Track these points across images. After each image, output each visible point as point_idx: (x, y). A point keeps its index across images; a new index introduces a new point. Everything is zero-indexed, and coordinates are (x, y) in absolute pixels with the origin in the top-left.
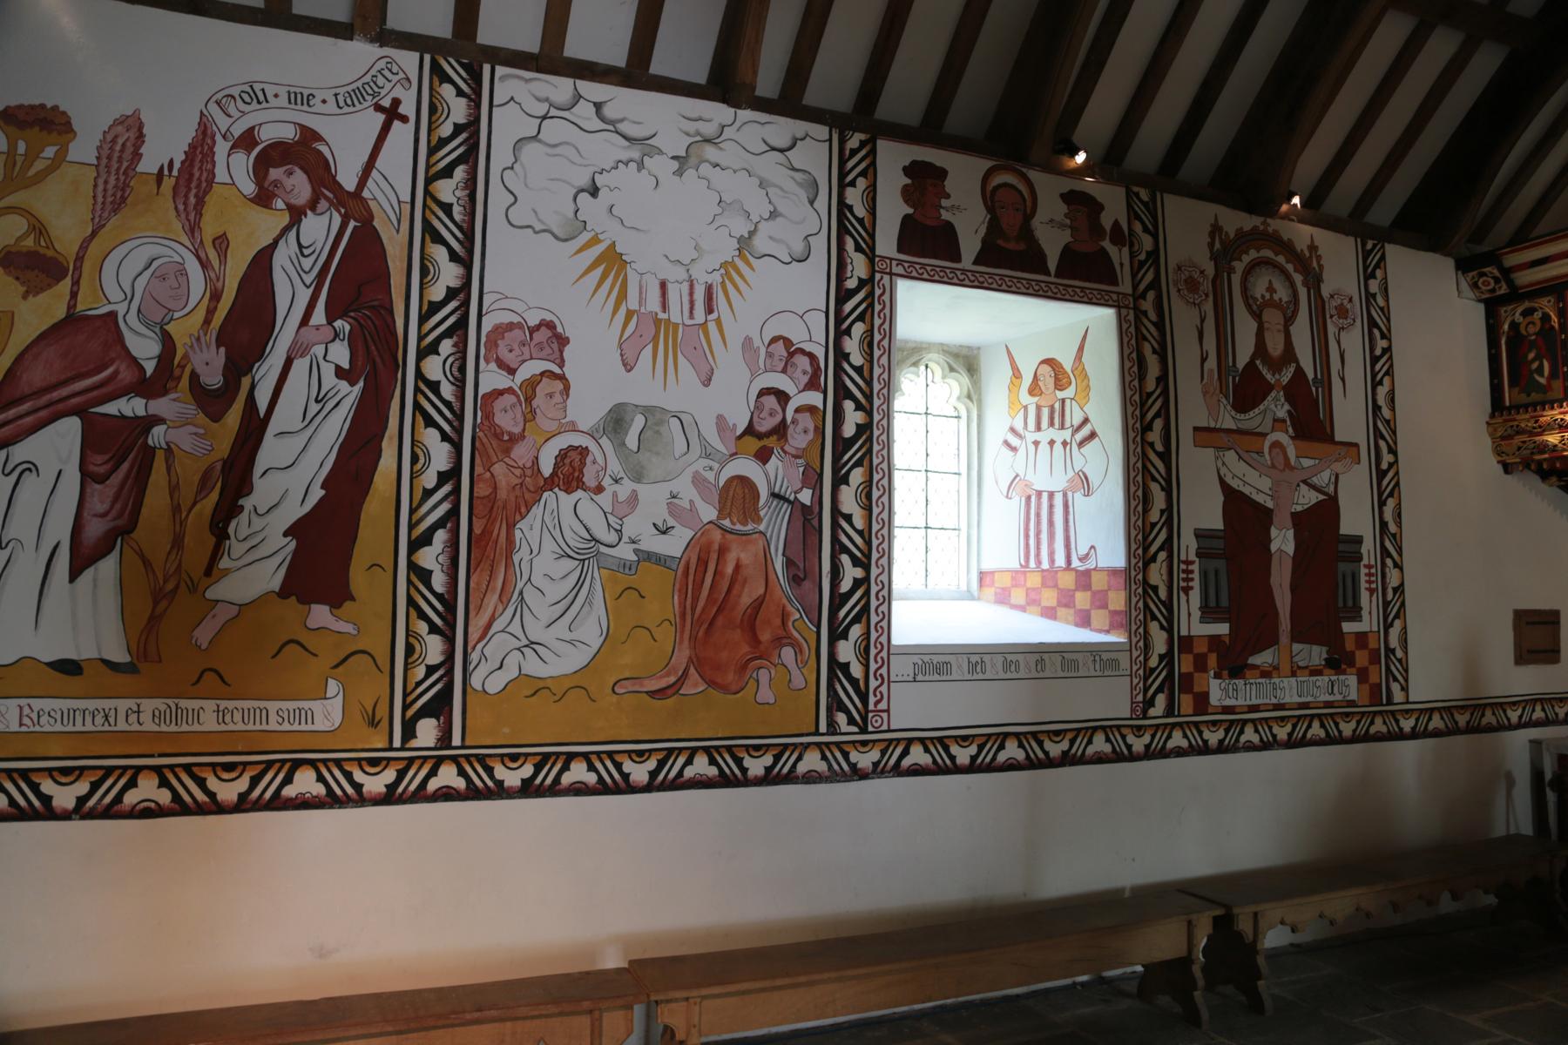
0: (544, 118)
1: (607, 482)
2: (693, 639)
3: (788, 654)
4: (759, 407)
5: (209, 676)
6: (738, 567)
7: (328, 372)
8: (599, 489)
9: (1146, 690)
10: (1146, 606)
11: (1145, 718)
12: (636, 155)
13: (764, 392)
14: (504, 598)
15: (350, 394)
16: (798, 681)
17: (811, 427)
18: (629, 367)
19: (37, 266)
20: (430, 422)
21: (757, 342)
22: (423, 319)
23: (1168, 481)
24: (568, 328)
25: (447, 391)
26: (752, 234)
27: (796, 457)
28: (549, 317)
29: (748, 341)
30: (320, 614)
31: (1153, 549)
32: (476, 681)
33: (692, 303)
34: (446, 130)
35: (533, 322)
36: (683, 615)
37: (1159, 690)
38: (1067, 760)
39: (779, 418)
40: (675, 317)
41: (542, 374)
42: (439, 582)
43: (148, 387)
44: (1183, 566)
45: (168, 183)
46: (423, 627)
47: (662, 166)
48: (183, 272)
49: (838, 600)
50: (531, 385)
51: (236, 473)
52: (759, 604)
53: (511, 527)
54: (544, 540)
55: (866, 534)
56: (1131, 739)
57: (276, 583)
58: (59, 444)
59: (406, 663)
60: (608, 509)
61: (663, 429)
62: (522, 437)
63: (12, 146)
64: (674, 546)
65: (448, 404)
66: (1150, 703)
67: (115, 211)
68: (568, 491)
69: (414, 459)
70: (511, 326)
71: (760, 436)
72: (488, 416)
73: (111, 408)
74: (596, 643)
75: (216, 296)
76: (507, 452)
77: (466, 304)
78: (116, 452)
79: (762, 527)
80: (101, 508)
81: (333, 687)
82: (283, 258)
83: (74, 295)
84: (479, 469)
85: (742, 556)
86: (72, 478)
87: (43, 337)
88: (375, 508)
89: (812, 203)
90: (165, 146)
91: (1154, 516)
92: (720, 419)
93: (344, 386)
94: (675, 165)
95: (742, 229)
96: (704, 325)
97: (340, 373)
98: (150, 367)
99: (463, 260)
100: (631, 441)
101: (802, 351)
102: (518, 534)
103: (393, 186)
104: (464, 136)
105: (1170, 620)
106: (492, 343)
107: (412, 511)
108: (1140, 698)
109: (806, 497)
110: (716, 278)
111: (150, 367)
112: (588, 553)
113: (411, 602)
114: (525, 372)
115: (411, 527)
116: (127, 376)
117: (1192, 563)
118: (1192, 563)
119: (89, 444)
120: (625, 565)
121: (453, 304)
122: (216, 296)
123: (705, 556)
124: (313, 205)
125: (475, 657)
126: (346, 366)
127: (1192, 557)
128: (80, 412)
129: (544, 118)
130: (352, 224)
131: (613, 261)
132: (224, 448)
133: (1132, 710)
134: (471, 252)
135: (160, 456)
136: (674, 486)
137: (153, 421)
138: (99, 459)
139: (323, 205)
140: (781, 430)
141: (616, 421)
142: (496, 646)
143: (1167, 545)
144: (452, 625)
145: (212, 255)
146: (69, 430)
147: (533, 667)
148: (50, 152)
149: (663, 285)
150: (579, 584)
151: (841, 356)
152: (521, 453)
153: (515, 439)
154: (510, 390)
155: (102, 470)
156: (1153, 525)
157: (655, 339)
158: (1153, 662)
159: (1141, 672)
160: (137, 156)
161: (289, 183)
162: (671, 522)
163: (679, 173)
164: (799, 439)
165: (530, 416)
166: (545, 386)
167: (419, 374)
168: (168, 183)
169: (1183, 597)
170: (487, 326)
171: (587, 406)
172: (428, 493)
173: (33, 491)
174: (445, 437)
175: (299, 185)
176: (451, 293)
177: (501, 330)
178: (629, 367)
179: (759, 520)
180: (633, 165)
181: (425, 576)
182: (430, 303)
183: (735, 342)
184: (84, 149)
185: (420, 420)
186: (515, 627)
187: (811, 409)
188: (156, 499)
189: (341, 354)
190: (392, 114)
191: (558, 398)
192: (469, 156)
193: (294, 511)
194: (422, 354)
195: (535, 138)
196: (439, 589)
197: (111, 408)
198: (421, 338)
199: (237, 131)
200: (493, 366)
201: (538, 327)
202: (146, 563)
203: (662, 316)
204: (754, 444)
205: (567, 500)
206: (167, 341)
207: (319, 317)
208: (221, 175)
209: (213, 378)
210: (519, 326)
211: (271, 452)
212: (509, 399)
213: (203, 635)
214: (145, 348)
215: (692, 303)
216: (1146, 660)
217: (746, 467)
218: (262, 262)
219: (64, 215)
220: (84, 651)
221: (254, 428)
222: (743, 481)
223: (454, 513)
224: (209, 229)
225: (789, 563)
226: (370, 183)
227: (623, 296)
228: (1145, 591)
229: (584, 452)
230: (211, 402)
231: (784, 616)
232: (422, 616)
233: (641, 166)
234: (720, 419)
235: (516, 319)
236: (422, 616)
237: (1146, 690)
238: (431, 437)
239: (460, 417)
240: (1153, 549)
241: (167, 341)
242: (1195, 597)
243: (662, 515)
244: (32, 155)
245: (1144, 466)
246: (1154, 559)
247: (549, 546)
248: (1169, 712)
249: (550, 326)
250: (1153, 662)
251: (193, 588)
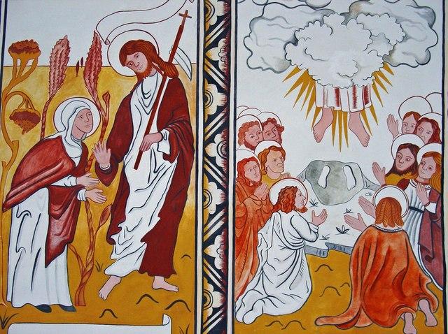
0: (266, 4)
1: (308, 205)
2: (363, 294)
3: (424, 304)
4: (399, 157)
5: (108, 313)
6: (389, 252)
7: (160, 156)
8: (304, 210)
12: (319, 16)
13: (401, 147)
14: (253, 271)
15: (171, 167)
16: (432, 321)
17: (434, 165)
18: (318, 139)
19: (27, 118)
20: (211, 179)
21: (397, 117)
22: (205, 125)
24: (282, 121)
25: (220, 162)
26: (391, 52)
27: (424, 184)
28: (272, 116)
29: (391, 118)
30: (159, 281)
32: (239, 317)
33: (355, 99)
34: (213, 21)
35: (264, 120)
36: (356, 280)
39: (412, 161)
40: (345, 107)
41: (270, 148)
42: (218, 263)
43: (77, 171)
45: (81, 70)
46: (211, 288)
47: (331, 20)
48: (90, 113)
50: (264, 155)
51: (118, 212)
52: (403, 274)
53: (256, 233)
54: (274, 238)
57: (138, 266)
58: (39, 202)
59: (203, 307)
60: (310, 220)
61: (340, 174)
62: (260, 183)
63: (15, 62)
64: (349, 240)
65: (220, 169)
67: (59, 87)
68: (287, 212)
69: (204, 199)
70: (252, 124)
71: (400, 173)
72: (242, 173)
73: (60, 183)
74: (305, 296)
75: (105, 124)
76: (252, 192)
77: (227, 114)
78: (64, 202)
79: (404, 228)
80: (58, 231)
81: (166, 319)
82: (135, 101)
83: (43, 130)
84: (238, 202)
85: (392, 245)
86: (46, 217)
87: (31, 151)
88: (184, 226)
89: (431, 26)
90: (79, 53)
92: (375, 165)
93: (167, 163)
94: (343, 18)
95: (385, 50)
96: (363, 111)
97: (165, 157)
98: (77, 161)
99: (225, 91)
100: (322, 182)
101: (426, 120)
102: (259, 236)
103: (187, 57)
104: (223, 22)
106: (242, 134)
107: (204, 226)
109: (432, 208)
110: (370, 82)
111: (77, 161)
112: (299, 246)
113: (204, 274)
114: (261, 147)
115: (203, 235)
116: (67, 167)
119: (52, 201)
120: (320, 251)
121: (221, 115)
122: (105, 124)
123: (368, 244)
124: (147, 73)
125: (238, 303)
126: (168, 153)
128: (48, 185)
129: (266, 4)
130: (168, 79)
131: (307, 81)
132: (112, 199)
134: (228, 86)
135: (83, 204)
136: (348, 206)
137: (79, 187)
138: (57, 207)
139: (154, 70)
140: (414, 169)
141: (312, 171)
142: (249, 297)
144: (226, 286)
145: (103, 103)
146: (44, 192)
147: (270, 310)
148: (30, 62)
149: (337, 91)
150: (294, 263)
152: (260, 192)
153: (256, 185)
154: (253, 159)
155: (58, 213)
157: (334, 122)
160: (67, 58)
161: (136, 61)
162: (347, 227)
163: (345, 23)
164: (426, 173)
165: (264, 172)
166: (272, 156)
167: (205, 154)
168: (81, 70)
170: (239, 125)
171: (295, 165)
172: (212, 216)
173: (30, 223)
174: (219, 186)
175: (141, 60)
176: (220, 109)
177: (247, 126)
178: (318, 139)
179: (402, 223)
180: (318, 23)
181: (211, 260)
182: (209, 115)
183: (383, 119)
184: (44, 59)
185: (206, 178)
186: (260, 288)
187: (434, 154)
188: (82, 225)
189: (165, 147)
190: (185, 16)
191: (279, 161)
192: (226, 34)
193: (145, 229)
194: (206, 144)
195: (261, 17)
196: (219, 267)
197: (60, 183)
198: (205, 135)
200: (243, 146)
201: (266, 123)
202: (78, 256)
203: (337, 108)
204: (397, 178)
205: (286, 217)
206: (84, 148)
207: (154, 129)
208: (105, 63)
209: (105, 165)
210: (256, 123)
211: (133, 200)
212: (253, 163)
213: (104, 292)
214: (74, 152)
215: (355, 99)
217: (393, 192)
218: (126, 103)
219: (36, 90)
220: (51, 301)
221: (124, 189)
222: (391, 201)
223: (225, 226)
224: (101, 90)
225: (423, 249)
226: (176, 56)
227: (314, 99)
229: (294, 189)
230: (105, 176)
231: (421, 281)
232: (211, 282)
233: (322, 22)
234: (375, 165)
235: (254, 119)
236: (211, 282)
238: (212, 187)
239: (227, 175)
241: (84, 148)
243: (341, 222)
244: (23, 65)
247: (277, 242)
249: (273, 121)
251: (99, 269)
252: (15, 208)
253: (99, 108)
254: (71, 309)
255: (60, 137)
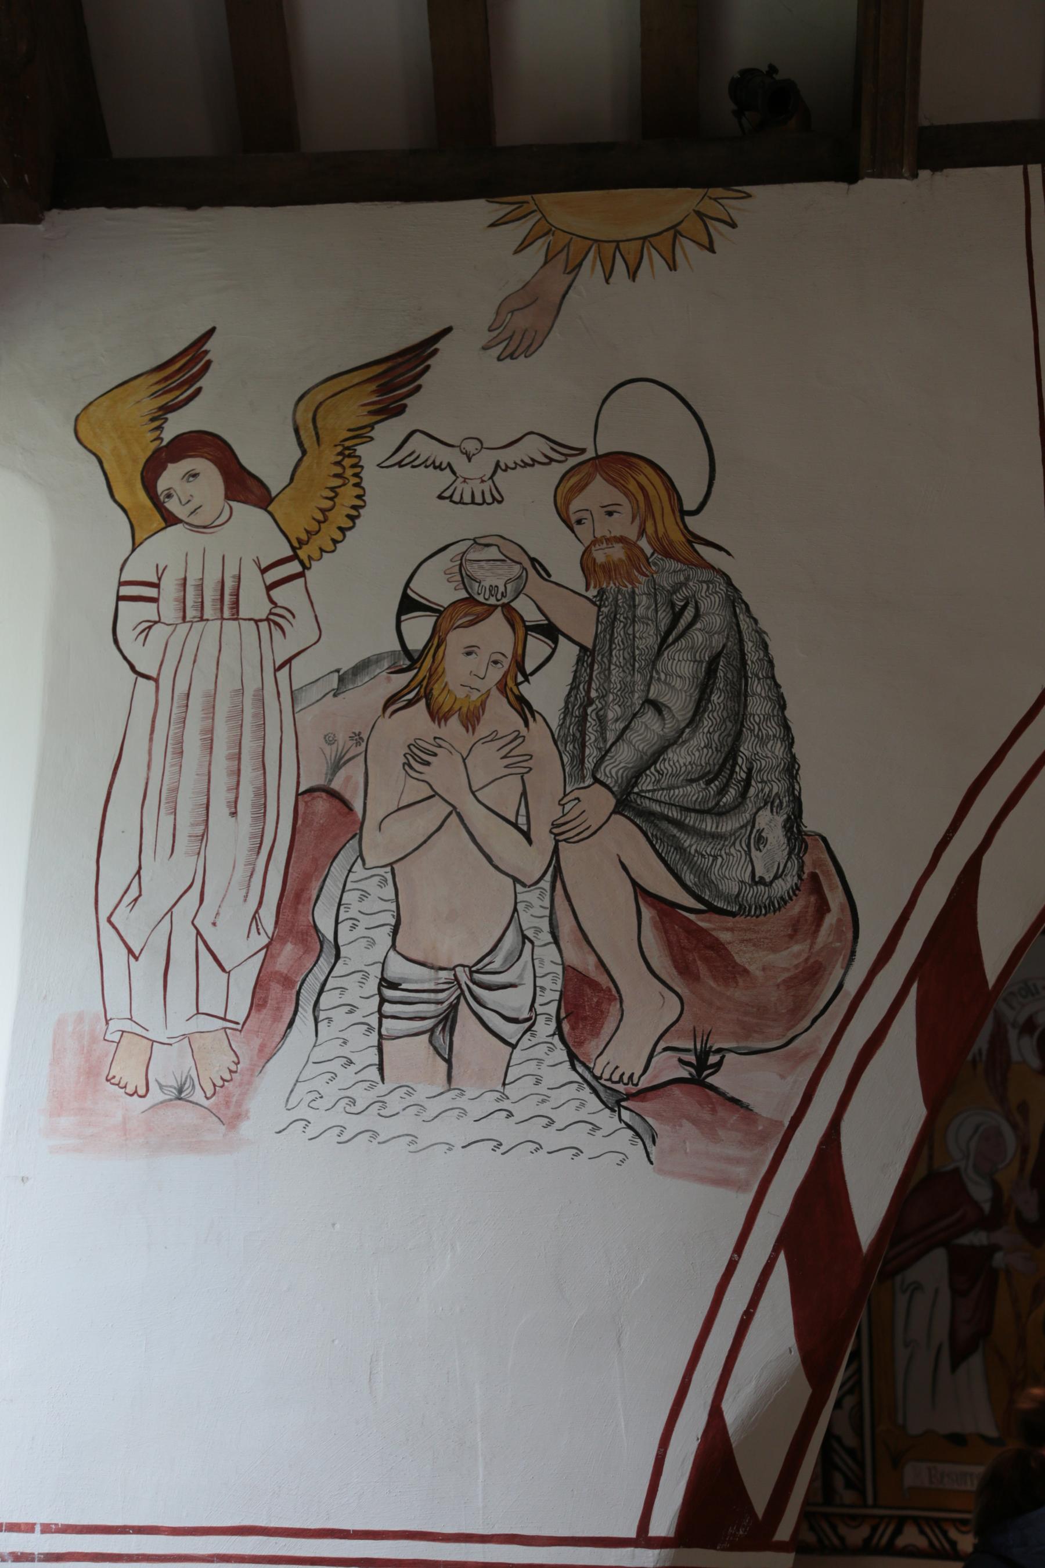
43: (990, 1222)
58: (933, 1269)
98: (987, 1207)
111: (987, 1207)
122: (1025, 1150)
137: (994, 1248)
199: (1022, 1019)
206: (996, 1187)
208: (1015, 1056)
214: (981, 1193)
241: (996, 1187)
252: (898, 1278)
253: (1015, 1127)
255: (956, 1171)
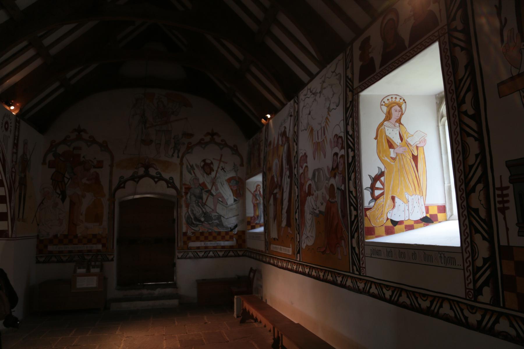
9: (475, 281)
10: (471, 223)
11: (475, 301)
23: (480, 132)
27: (340, 174)
31: (472, 183)
37: (486, 283)
38: (428, 312)
44: (498, 192)
49: (352, 223)
55: (356, 197)
56: (466, 313)
66: (479, 292)
91: (471, 160)
105: (490, 232)
108: (471, 286)
117: (507, 188)
118: (507, 188)
127: (506, 183)
133: (467, 294)
143: (483, 178)
151: (347, 133)
156: (471, 167)
158: (479, 263)
159: (471, 268)
169: (500, 216)
216: (474, 260)
228: (468, 212)
234: (328, 167)
237: (475, 281)
240: (472, 183)
242: (512, 215)
245: (462, 129)
246: (473, 190)
248: (495, 301)
250: (479, 263)
254: (277, 240)
